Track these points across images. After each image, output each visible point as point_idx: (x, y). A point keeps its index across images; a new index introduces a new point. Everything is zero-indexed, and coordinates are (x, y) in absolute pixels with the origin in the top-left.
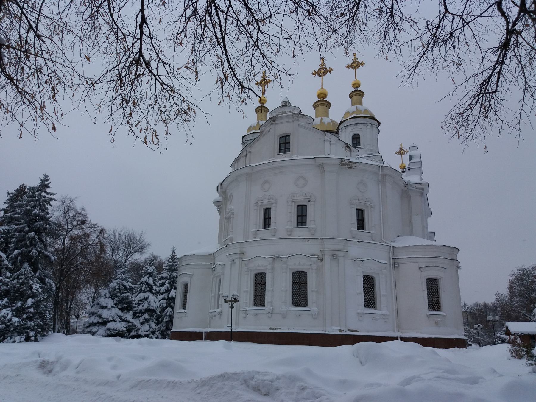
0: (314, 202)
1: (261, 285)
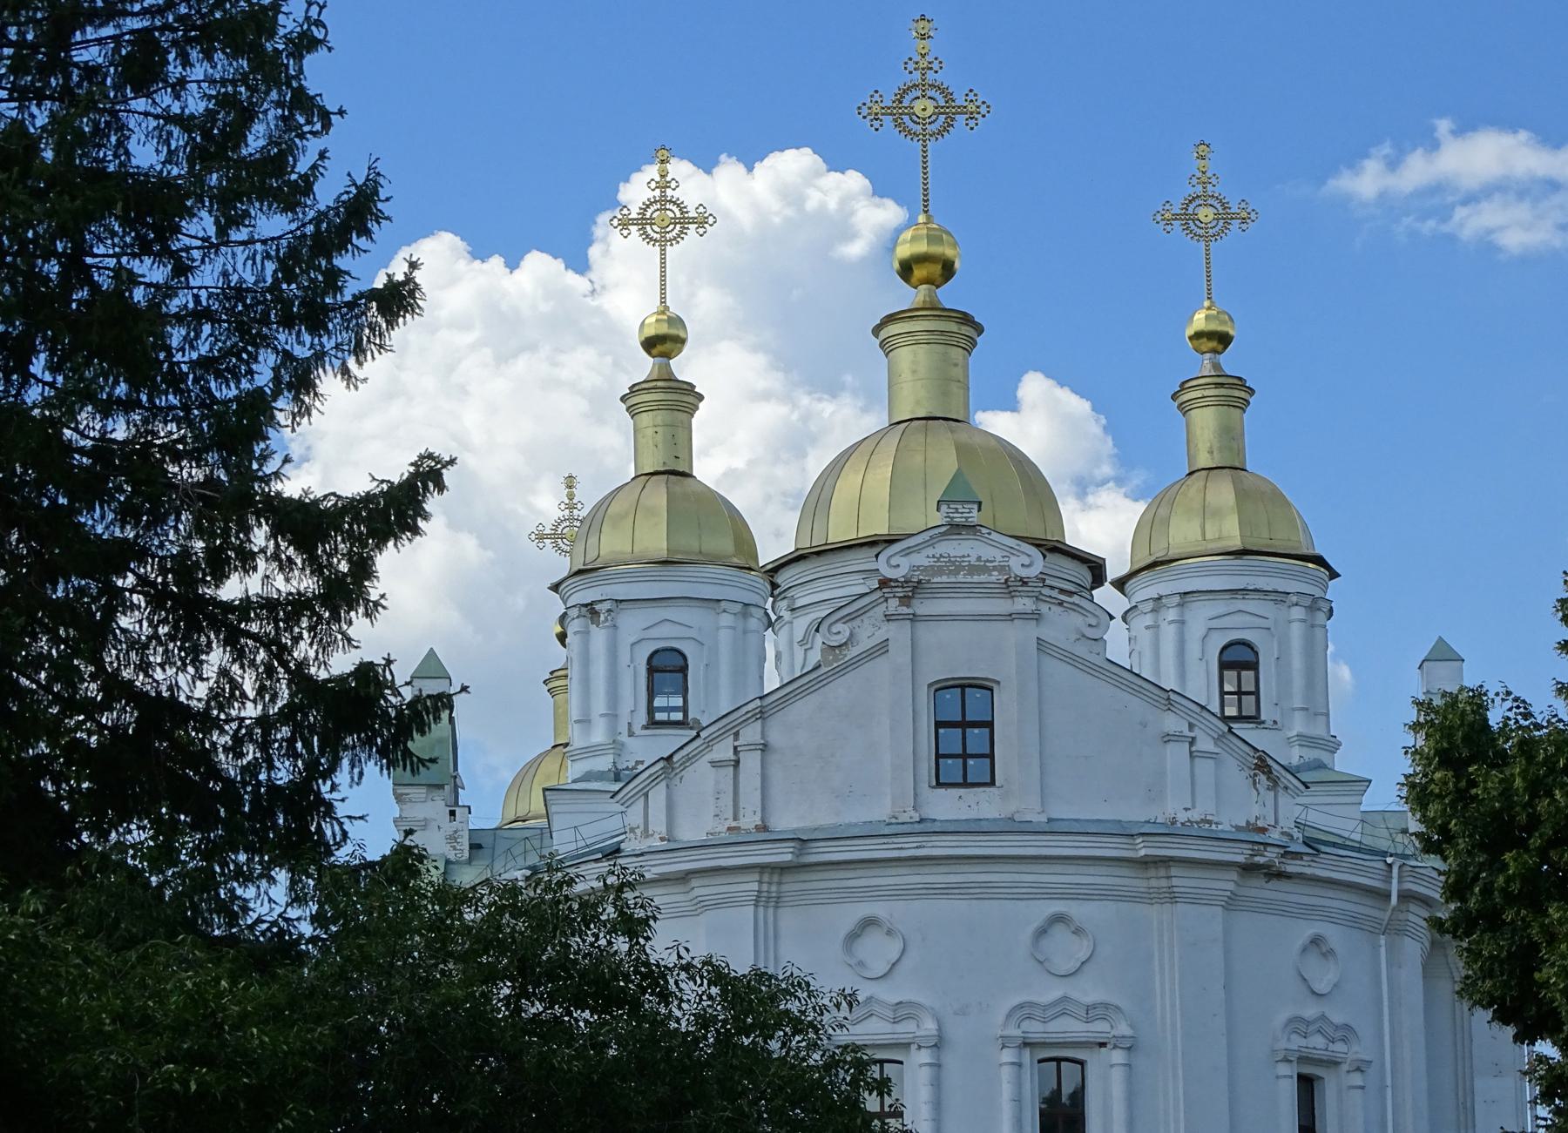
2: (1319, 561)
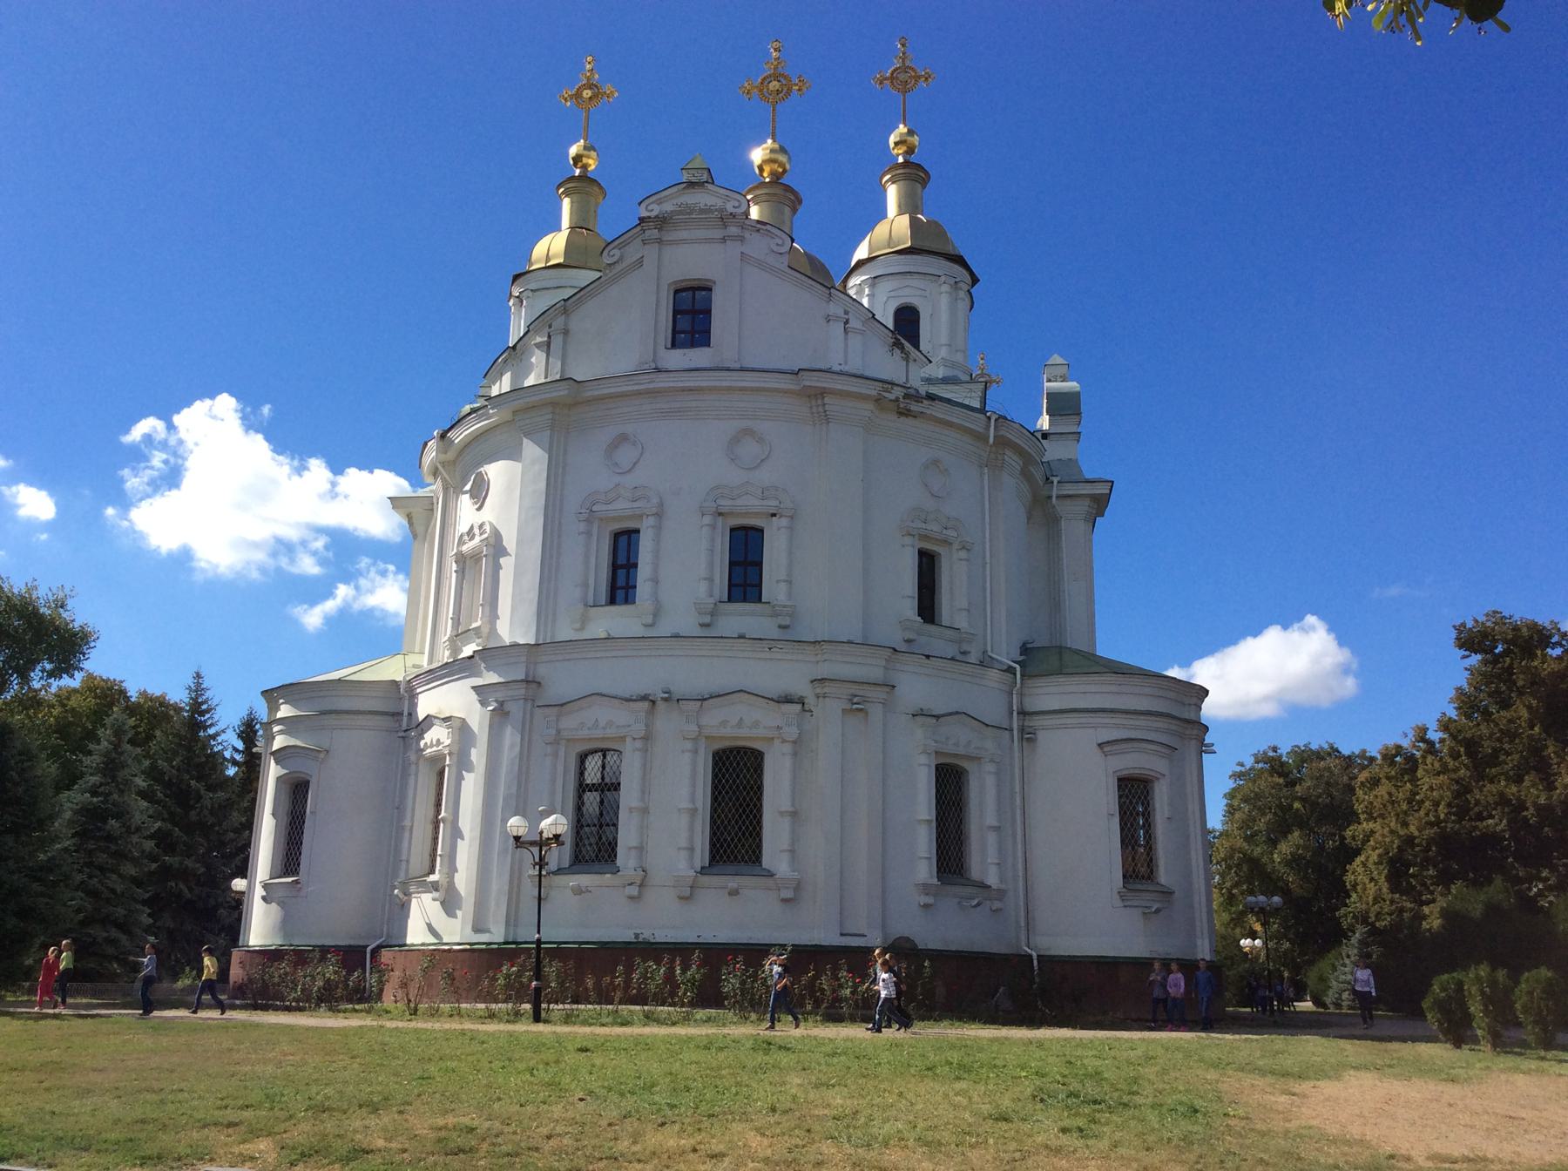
0: (792, 517)
1: (602, 791)
2: (959, 260)
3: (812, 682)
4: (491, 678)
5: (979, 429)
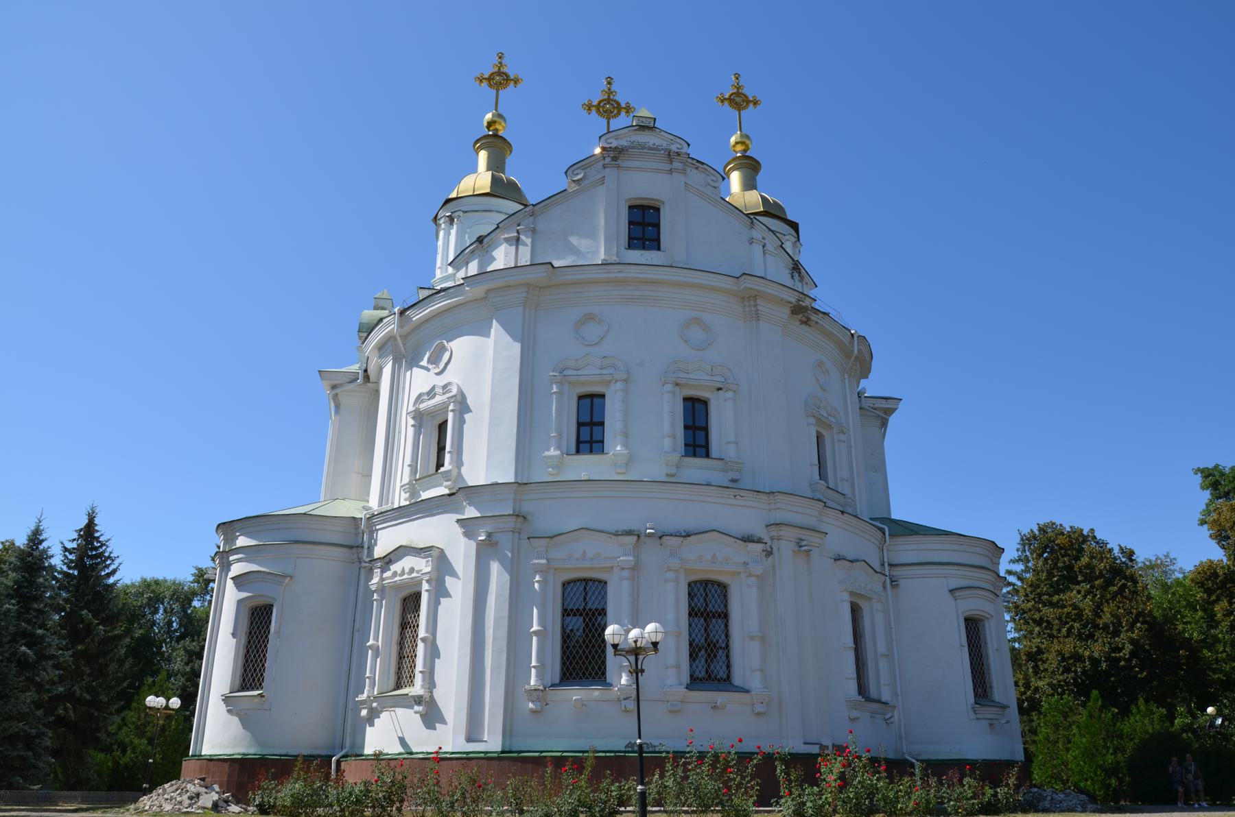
3: (767, 526)
4: (471, 512)
5: (846, 342)
